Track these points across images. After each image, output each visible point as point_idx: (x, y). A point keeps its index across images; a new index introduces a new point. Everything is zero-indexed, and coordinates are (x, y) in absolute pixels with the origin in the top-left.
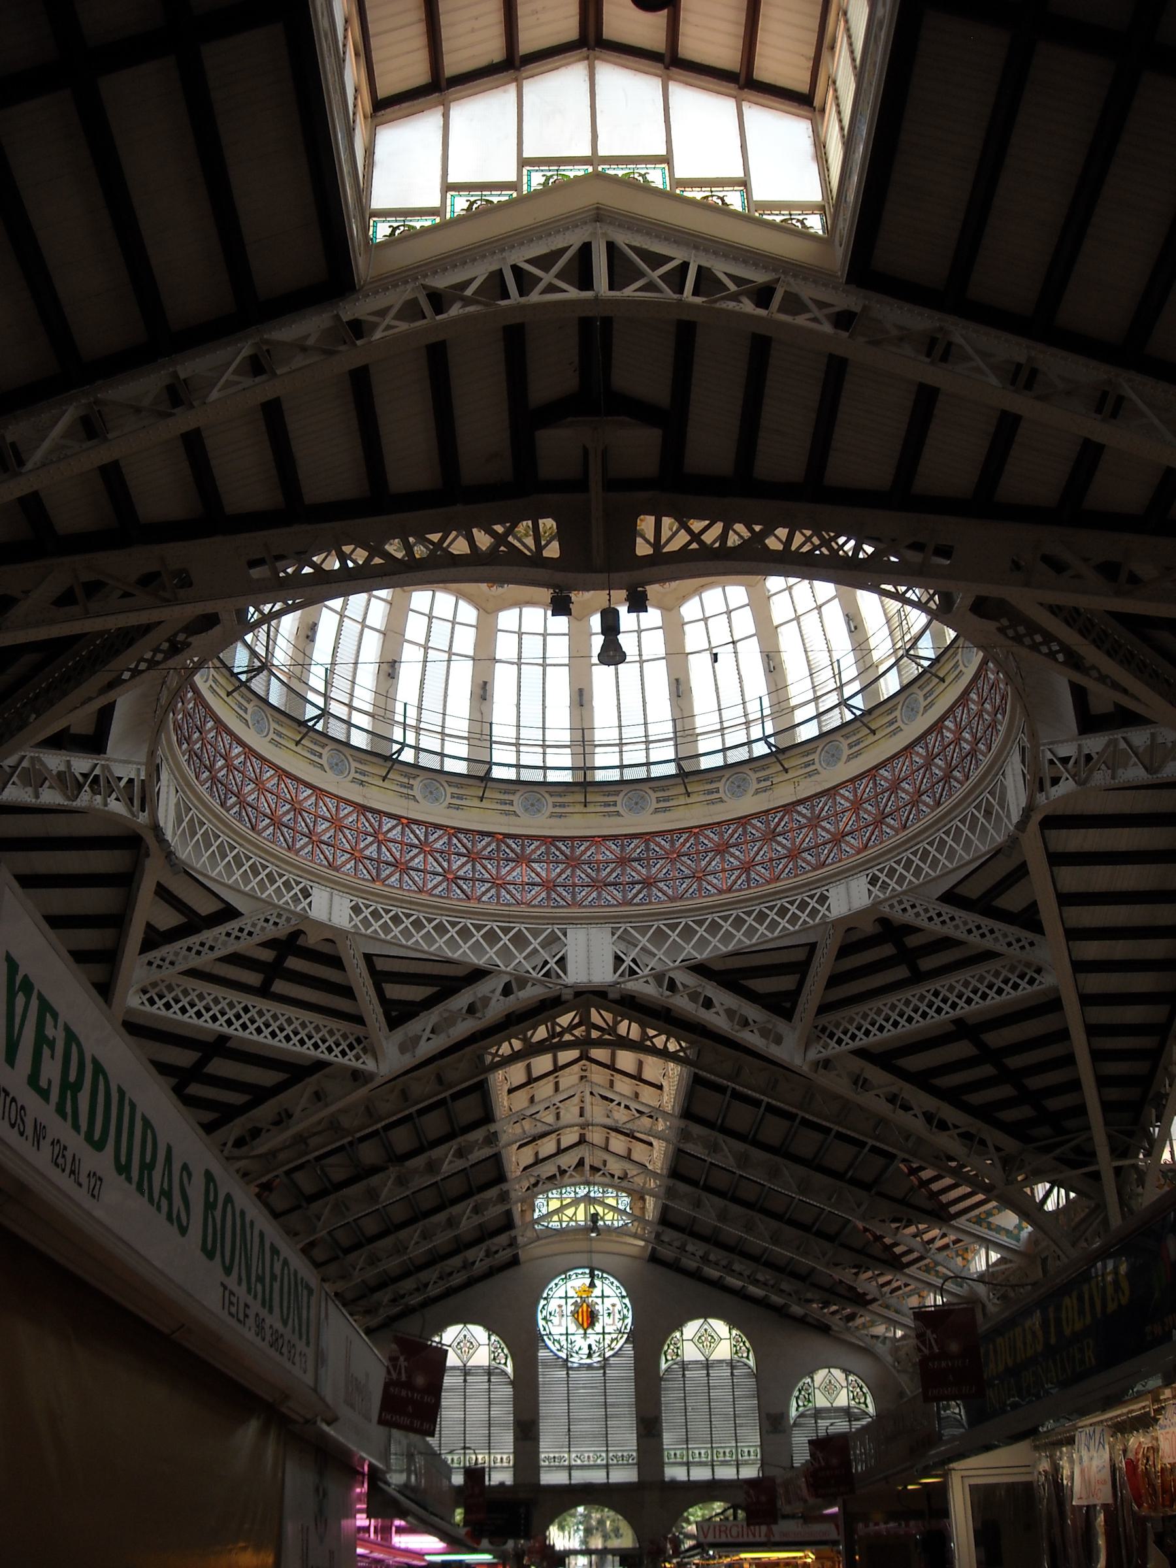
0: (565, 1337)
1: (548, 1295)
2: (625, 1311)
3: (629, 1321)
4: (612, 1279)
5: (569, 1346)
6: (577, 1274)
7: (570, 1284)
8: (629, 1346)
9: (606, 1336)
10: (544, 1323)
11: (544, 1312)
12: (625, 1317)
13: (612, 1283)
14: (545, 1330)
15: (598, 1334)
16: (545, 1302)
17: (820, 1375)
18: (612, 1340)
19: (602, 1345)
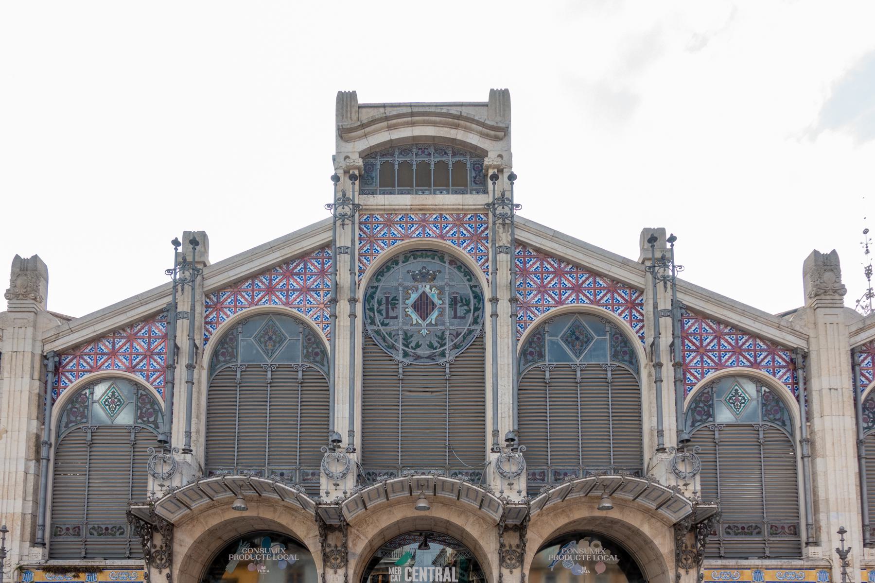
10: (371, 314)
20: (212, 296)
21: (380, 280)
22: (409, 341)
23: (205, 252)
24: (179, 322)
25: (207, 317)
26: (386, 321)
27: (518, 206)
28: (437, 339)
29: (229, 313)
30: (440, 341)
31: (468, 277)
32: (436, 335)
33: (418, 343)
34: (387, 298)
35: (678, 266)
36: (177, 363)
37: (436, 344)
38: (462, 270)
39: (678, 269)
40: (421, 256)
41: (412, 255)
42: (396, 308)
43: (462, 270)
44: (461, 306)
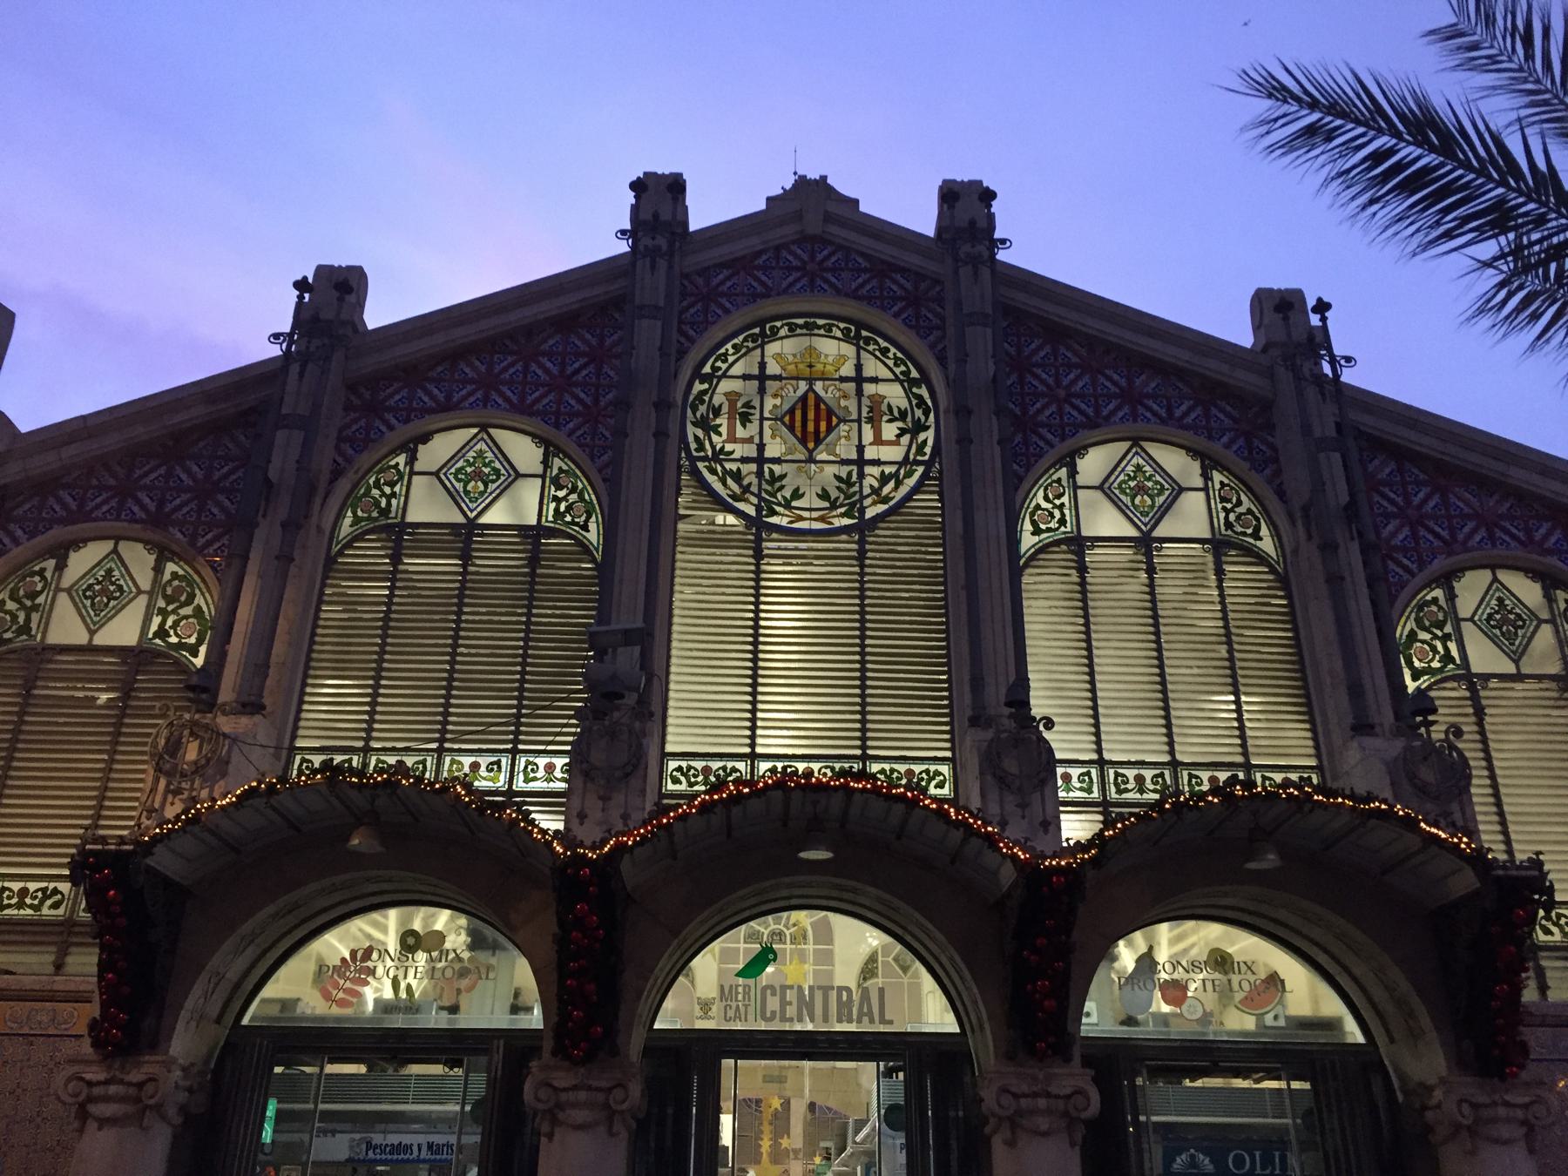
0: (753, 467)
1: (715, 369)
2: (919, 413)
3: (929, 436)
4: (884, 344)
5: (765, 486)
6: (793, 327)
7: (773, 348)
8: (928, 501)
9: (868, 470)
10: (700, 433)
11: (702, 409)
12: (919, 427)
13: (885, 351)
14: (701, 448)
15: (844, 462)
16: (706, 386)
17: (1471, 590)
18: (884, 479)
19: (856, 488)
20: (363, 390)
21: (720, 368)
22: (778, 485)
23: (361, 305)
24: (281, 435)
25: (348, 426)
26: (728, 447)
27: (1003, 241)
28: (837, 484)
29: (393, 421)
30: (843, 486)
31: (903, 368)
32: (838, 478)
33: (797, 489)
34: (732, 404)
35: (1343, 357)
36: (264, 516)
37: (834, 494)
38: (891, 355)
39: (1343, 362)
40: (806, 326)
41: (787, 324)
42: (750, 422)
43: (891, 355)
44: (890, 421)
